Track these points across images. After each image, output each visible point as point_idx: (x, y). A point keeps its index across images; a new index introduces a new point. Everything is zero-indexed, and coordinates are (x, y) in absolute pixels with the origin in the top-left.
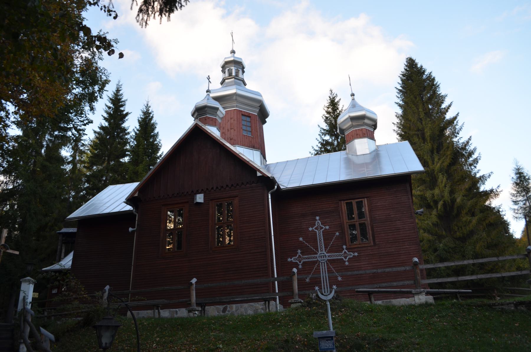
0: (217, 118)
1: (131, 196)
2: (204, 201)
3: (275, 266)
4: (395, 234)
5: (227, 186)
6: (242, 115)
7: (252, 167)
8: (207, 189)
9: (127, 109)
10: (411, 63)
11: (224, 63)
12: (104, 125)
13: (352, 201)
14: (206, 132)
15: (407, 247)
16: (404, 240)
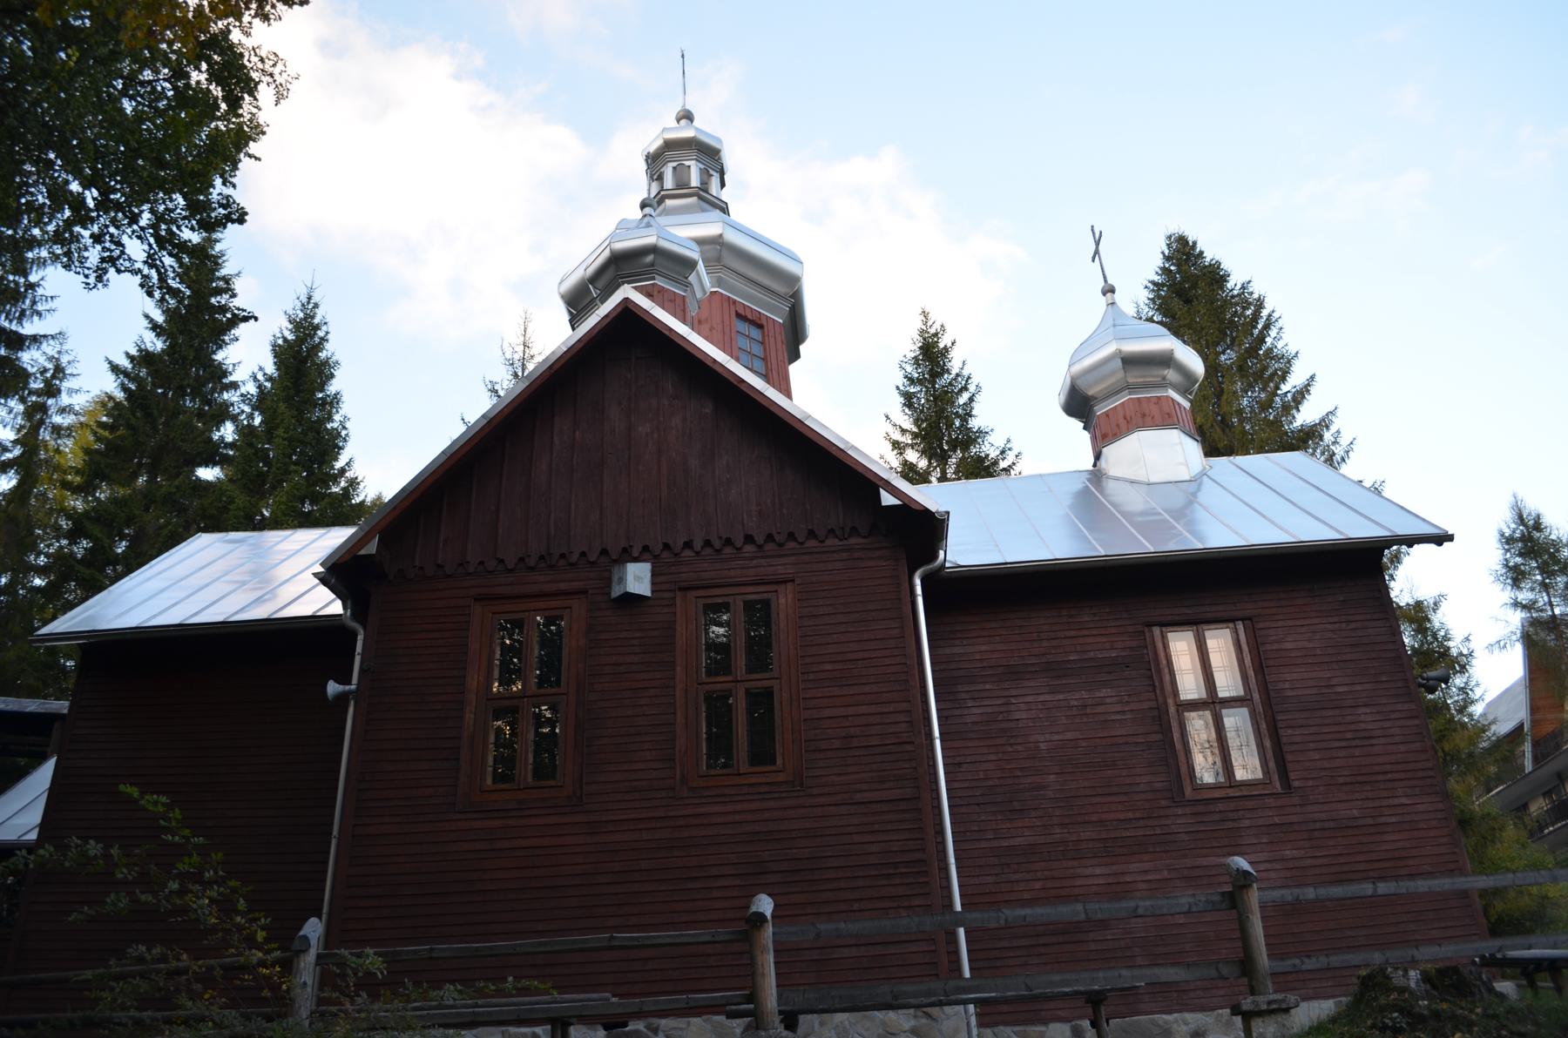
1: (348, 551)
2: (653, 592)
4: (1357, 752)
6: (738, 315)
7: (860, 470)
8: (666, 546)
11: (659, 142)
12: (151, 349)
14: (667, 333)
15: (1404, 801)
16: (1389, 776)
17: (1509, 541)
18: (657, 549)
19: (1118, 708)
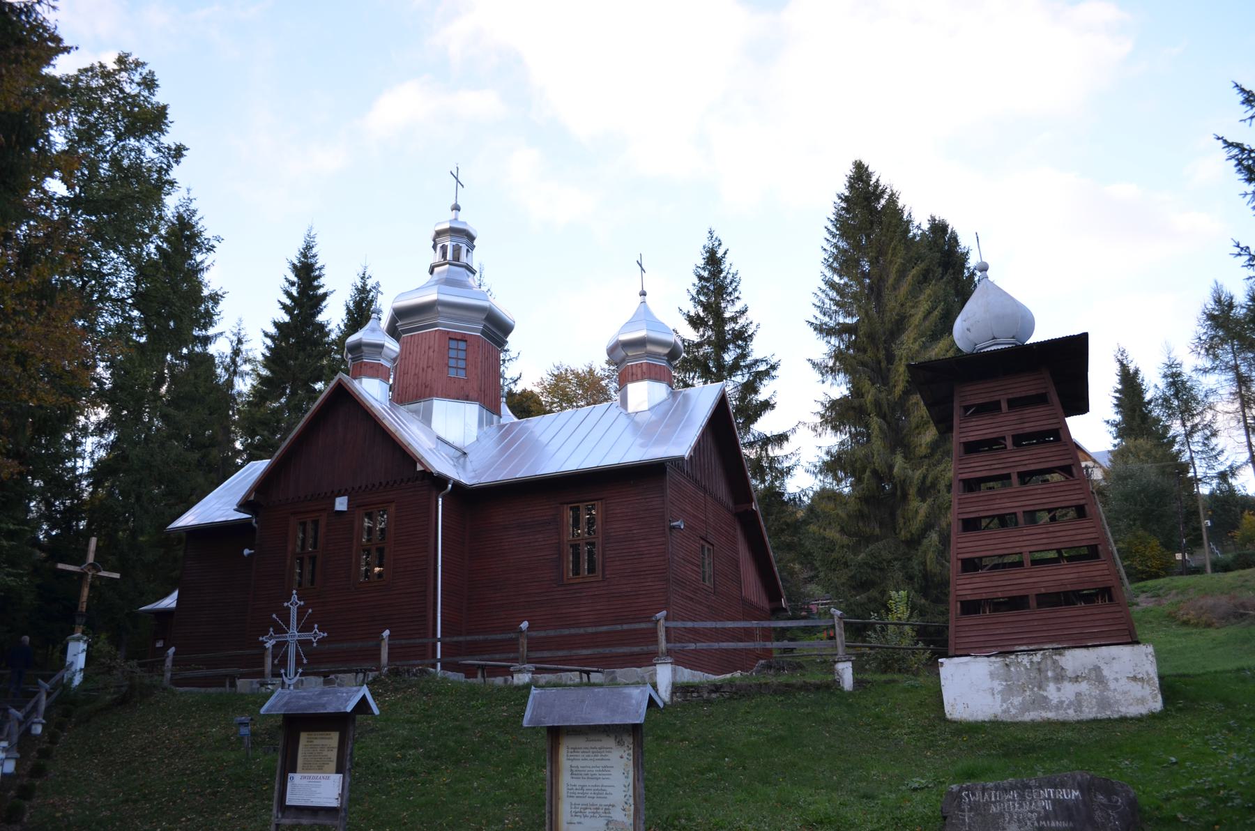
0: (383, 362)
3: (439, 615)
9: (327, 282)
10: (860, 174)
13: (580, 505)
15: (650, 584)
17: (1211, 317)
19: (543, 543)
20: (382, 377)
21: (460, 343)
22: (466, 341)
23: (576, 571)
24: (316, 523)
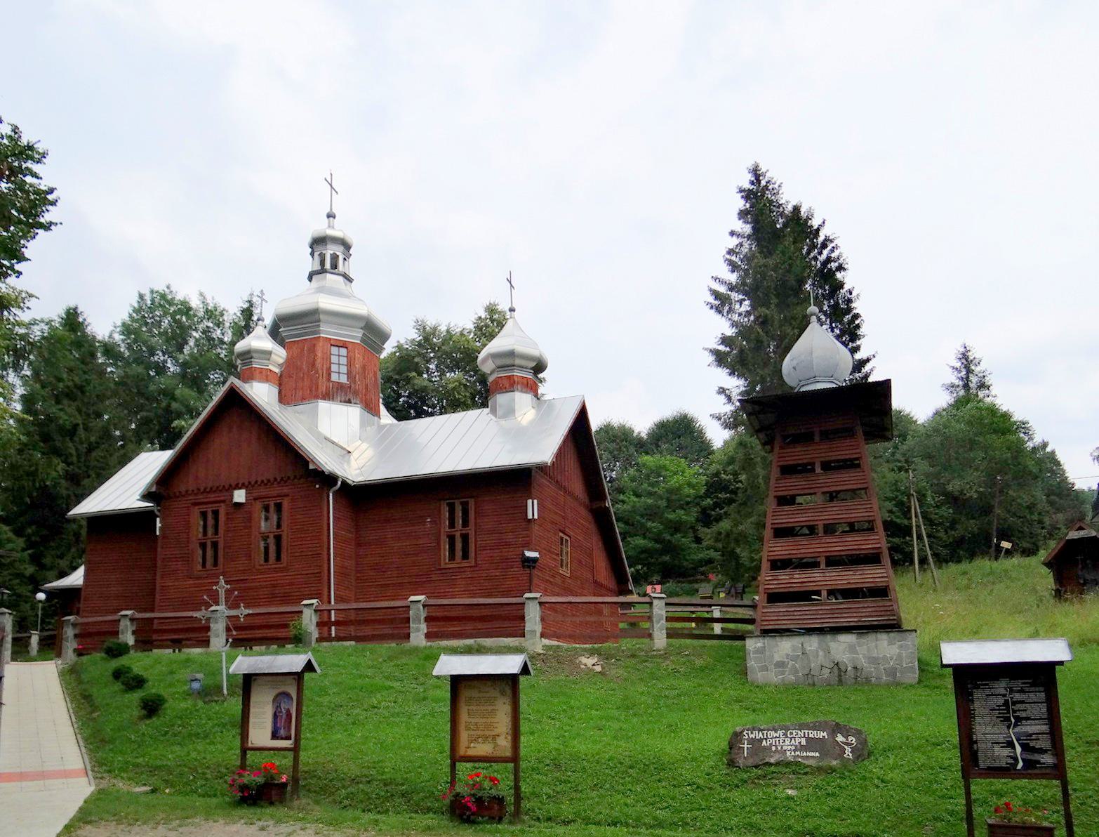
0: (271, 367)
5: (275, 479)
18: (246, 484)
20: (271, 382)
21: (341, 349)
22: (346, 348)
23: (452, 557)
24: (216, 513)
